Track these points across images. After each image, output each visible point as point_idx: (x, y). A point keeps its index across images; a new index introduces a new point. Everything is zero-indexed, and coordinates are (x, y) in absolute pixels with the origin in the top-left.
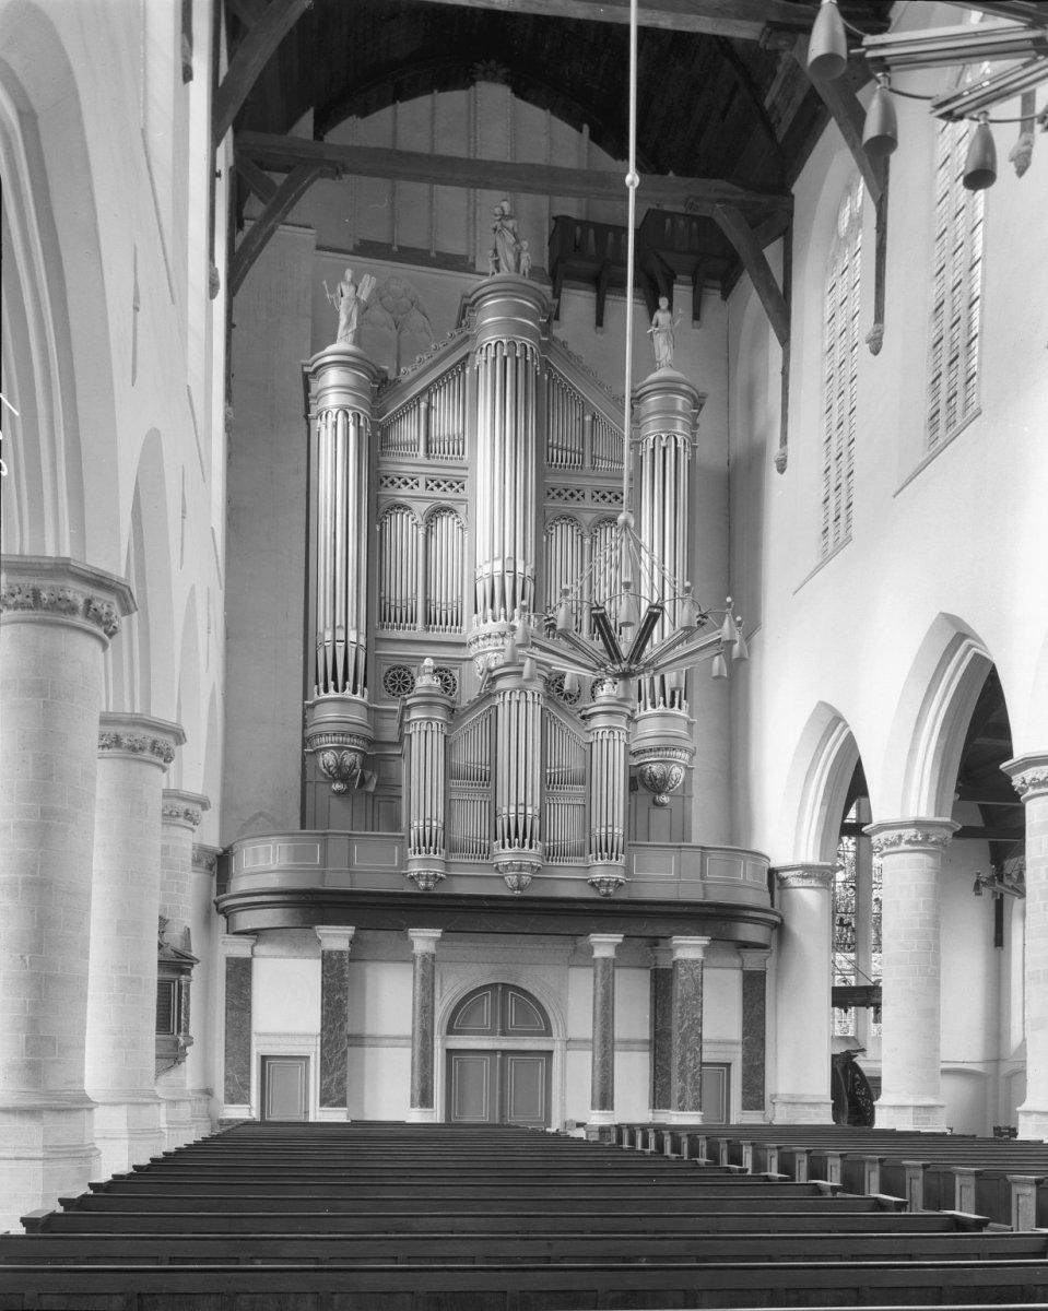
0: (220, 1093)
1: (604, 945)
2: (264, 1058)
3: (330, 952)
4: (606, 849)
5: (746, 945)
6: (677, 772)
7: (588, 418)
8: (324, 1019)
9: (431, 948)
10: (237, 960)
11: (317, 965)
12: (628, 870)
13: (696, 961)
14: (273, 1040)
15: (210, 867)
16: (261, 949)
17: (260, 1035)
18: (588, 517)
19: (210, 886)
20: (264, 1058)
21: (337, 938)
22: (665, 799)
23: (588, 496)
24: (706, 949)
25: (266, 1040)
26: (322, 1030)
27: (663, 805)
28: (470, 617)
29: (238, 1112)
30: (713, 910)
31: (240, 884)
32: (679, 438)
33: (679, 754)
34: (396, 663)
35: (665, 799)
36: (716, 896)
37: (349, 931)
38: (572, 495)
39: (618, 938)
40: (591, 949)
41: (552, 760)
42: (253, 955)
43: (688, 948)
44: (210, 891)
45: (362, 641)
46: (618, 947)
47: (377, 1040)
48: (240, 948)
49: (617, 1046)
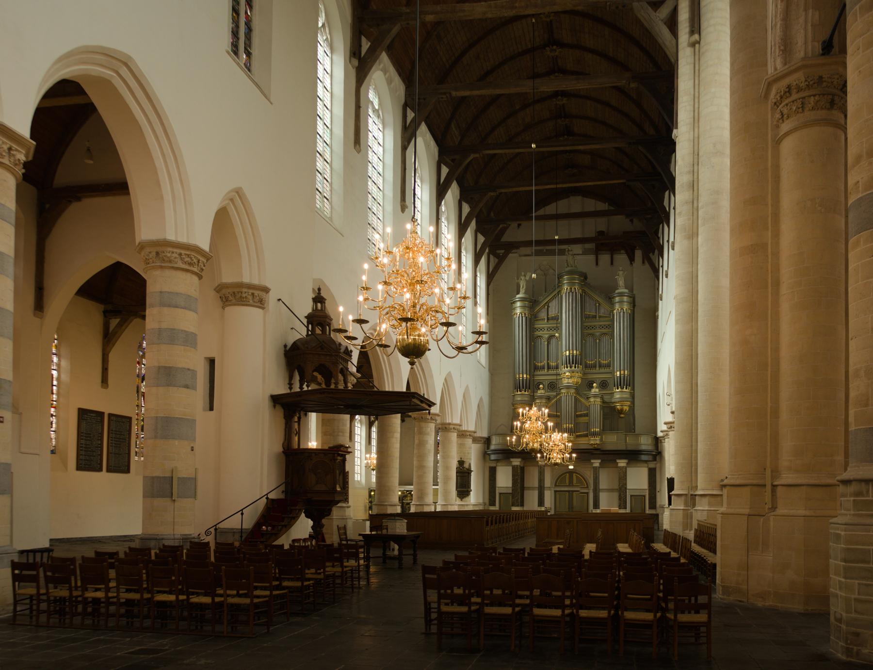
1: (596, 463)
2: (500, 494)
3: (514, 466)
4: (594, 434)
6: (626, 408)
7: (597, 305)
8: (513, 483)
10: (492, 467)
11: (511, 468)
12: (601, 440)
14: (501, 489)
17: (499, 487)
18: (598, 334)
20: (500, 494)
21: (516, 462)
22: (622, 416)
23: (598, 327)
25: (499, 489)
26: (513, 486)
27: (621, 417)
28: (561, 367)
29: (492, 508)
30: (628, 452)
32: (624, 309)
33: (627, 403)
34: (539, 381)
35: (622, 416)
36: (630, 448)
38: (593, 328)
39: (599, 461)
40: (593, 463)
46: (600, 464)
47: (529, 488)
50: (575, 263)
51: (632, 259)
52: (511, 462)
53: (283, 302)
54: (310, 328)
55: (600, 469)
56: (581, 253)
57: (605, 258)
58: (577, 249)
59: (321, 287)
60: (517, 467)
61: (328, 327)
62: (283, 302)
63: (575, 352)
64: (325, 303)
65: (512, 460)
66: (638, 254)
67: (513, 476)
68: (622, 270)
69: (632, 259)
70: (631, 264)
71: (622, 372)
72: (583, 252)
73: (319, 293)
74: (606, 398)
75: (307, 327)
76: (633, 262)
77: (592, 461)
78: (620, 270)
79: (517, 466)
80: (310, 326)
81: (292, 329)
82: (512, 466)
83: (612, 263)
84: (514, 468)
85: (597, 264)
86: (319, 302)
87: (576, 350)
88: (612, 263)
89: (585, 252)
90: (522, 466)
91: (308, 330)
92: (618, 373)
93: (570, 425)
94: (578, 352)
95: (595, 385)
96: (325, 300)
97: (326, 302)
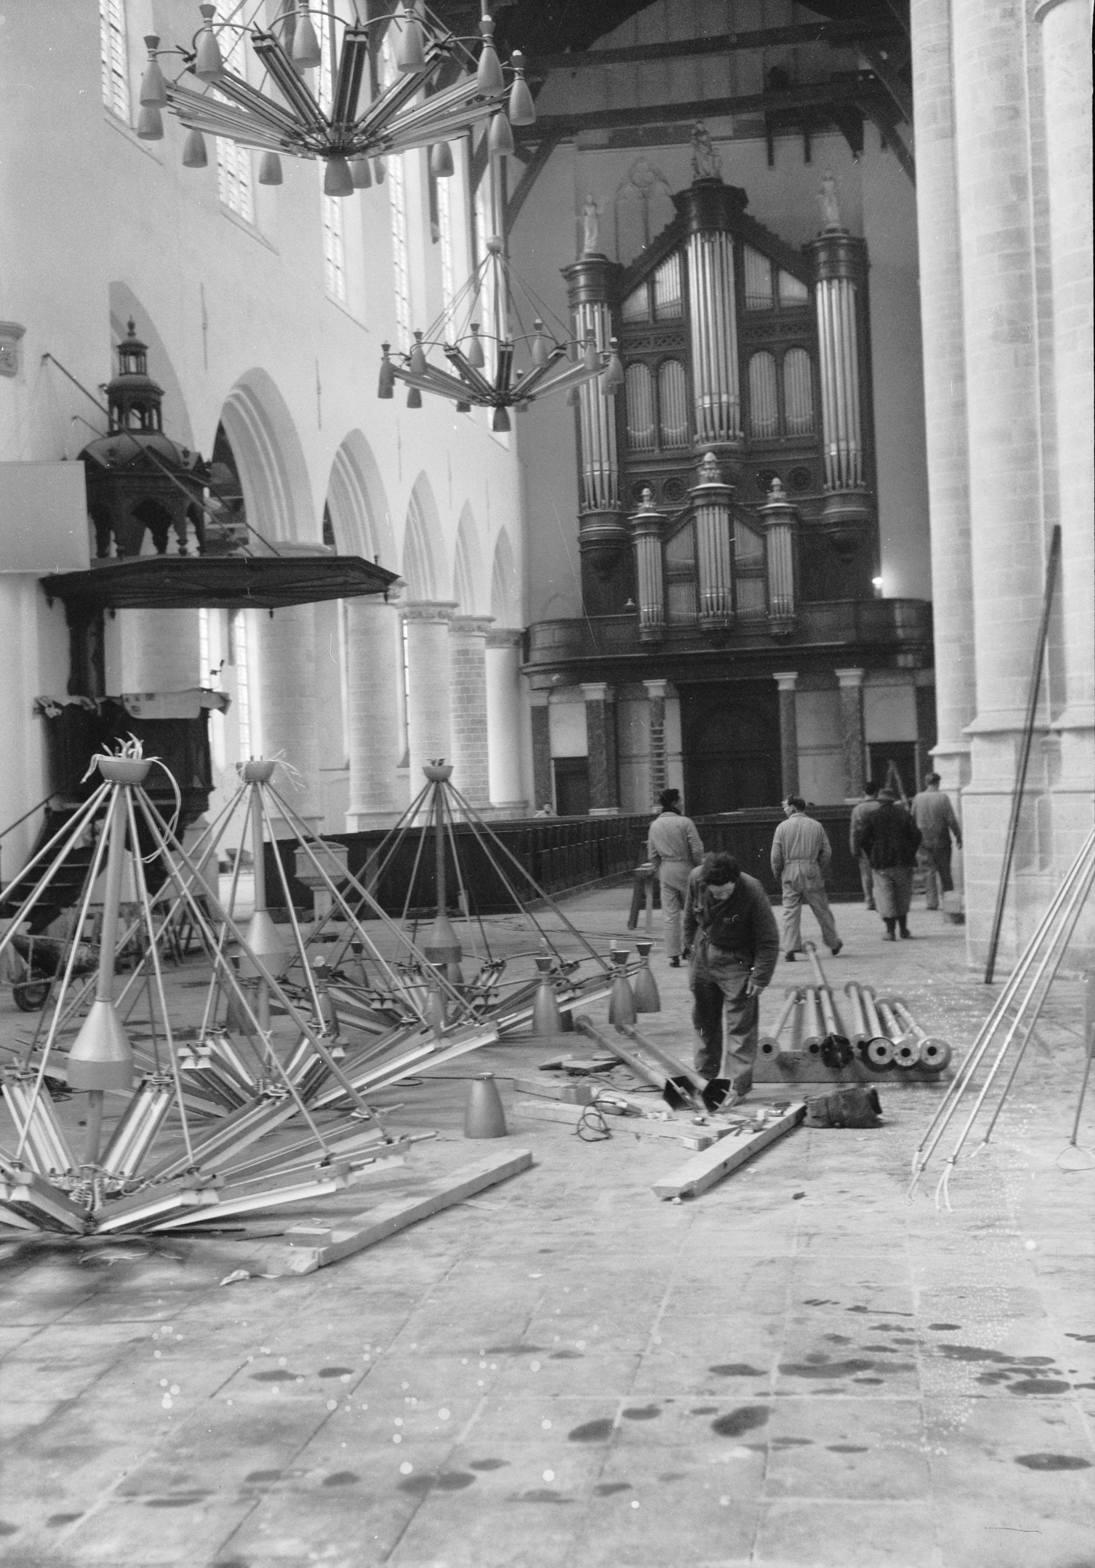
0: (532, 803)
5: (907, 670)
9: (661, 693)
13: (853, 687)
15: (517, 643)
16: (554, 699)
19: (518, 657)
21: (596, 691)
24: (864, 678)
31: (536, 657)
37: (602, 686)
39: (793, 675)
41: (738, 550)
42: (549, 703)
43: (849, 677)
44: (517, 662)
45: (615, 467)
46: (797, 682)
48: (540, 700)
49: (800, 752)
50: (717, 165)
51: (857, 146)
52: (582, 692)
53: (55, 361)
54: (115, 417)
55: (798, 696)
56: (730, 133)
57: (790, 146)
58: (719, 125)
59: (135, 320)
60: (598, 706)
61: (154, 412)
62: (55, 361)
63: (724, 398)
64: (144, 355)
65: (585, 686)
66: (871, 132)
67: (590, 727)
68: (831, 178)
69: (857, 146)
70: (855, 156)
71: (843, 445)
72: (735, 131)
73: (131, 334)
74: (808, 516)
75: (110, 413)
76: (858, 153)
77: (777, 676)
78: (825, 179)
79: (598, 701)
80: (116, 411)
81: (75, 418)
82: (586, 702)
83: (808, 159)
84: (591, 706)
85: (771, 162)
86: (133, 354)
87: (727, 392)
88: (808, 159)
89: (741, 132)
90: (610, 700)
91: (111, 422)
92: (834, 447)
93: (720, 590)
94: (732, 400)
95: (776, 481)
96: (146, 348)
97: (148, 352)
